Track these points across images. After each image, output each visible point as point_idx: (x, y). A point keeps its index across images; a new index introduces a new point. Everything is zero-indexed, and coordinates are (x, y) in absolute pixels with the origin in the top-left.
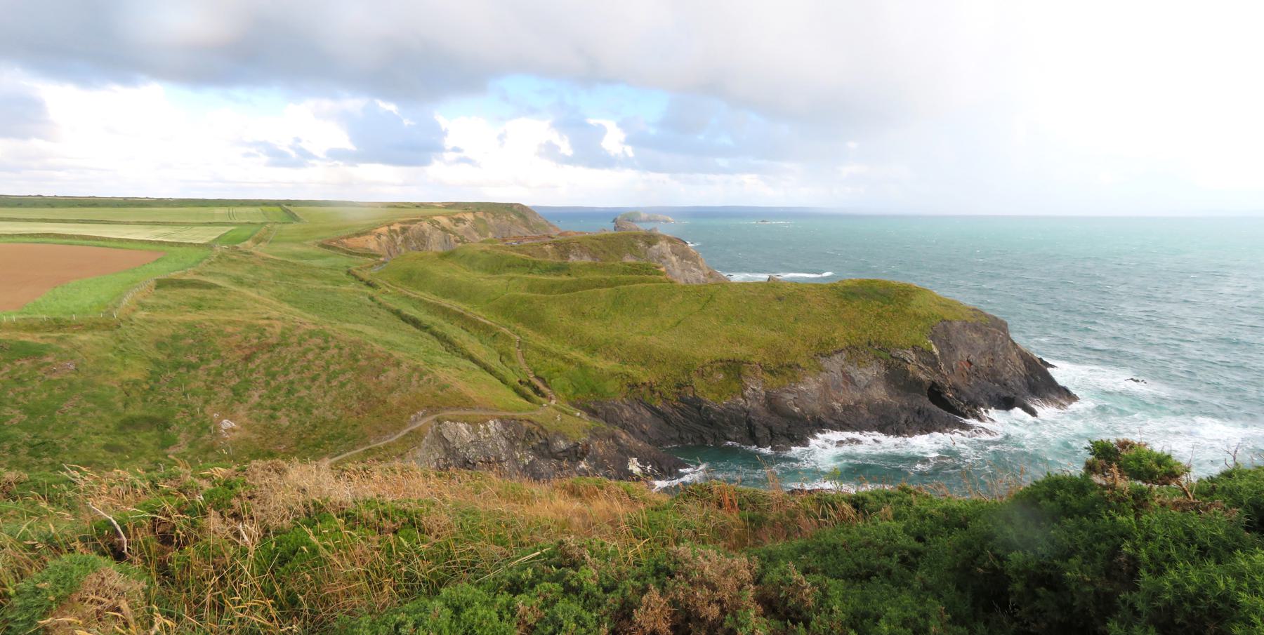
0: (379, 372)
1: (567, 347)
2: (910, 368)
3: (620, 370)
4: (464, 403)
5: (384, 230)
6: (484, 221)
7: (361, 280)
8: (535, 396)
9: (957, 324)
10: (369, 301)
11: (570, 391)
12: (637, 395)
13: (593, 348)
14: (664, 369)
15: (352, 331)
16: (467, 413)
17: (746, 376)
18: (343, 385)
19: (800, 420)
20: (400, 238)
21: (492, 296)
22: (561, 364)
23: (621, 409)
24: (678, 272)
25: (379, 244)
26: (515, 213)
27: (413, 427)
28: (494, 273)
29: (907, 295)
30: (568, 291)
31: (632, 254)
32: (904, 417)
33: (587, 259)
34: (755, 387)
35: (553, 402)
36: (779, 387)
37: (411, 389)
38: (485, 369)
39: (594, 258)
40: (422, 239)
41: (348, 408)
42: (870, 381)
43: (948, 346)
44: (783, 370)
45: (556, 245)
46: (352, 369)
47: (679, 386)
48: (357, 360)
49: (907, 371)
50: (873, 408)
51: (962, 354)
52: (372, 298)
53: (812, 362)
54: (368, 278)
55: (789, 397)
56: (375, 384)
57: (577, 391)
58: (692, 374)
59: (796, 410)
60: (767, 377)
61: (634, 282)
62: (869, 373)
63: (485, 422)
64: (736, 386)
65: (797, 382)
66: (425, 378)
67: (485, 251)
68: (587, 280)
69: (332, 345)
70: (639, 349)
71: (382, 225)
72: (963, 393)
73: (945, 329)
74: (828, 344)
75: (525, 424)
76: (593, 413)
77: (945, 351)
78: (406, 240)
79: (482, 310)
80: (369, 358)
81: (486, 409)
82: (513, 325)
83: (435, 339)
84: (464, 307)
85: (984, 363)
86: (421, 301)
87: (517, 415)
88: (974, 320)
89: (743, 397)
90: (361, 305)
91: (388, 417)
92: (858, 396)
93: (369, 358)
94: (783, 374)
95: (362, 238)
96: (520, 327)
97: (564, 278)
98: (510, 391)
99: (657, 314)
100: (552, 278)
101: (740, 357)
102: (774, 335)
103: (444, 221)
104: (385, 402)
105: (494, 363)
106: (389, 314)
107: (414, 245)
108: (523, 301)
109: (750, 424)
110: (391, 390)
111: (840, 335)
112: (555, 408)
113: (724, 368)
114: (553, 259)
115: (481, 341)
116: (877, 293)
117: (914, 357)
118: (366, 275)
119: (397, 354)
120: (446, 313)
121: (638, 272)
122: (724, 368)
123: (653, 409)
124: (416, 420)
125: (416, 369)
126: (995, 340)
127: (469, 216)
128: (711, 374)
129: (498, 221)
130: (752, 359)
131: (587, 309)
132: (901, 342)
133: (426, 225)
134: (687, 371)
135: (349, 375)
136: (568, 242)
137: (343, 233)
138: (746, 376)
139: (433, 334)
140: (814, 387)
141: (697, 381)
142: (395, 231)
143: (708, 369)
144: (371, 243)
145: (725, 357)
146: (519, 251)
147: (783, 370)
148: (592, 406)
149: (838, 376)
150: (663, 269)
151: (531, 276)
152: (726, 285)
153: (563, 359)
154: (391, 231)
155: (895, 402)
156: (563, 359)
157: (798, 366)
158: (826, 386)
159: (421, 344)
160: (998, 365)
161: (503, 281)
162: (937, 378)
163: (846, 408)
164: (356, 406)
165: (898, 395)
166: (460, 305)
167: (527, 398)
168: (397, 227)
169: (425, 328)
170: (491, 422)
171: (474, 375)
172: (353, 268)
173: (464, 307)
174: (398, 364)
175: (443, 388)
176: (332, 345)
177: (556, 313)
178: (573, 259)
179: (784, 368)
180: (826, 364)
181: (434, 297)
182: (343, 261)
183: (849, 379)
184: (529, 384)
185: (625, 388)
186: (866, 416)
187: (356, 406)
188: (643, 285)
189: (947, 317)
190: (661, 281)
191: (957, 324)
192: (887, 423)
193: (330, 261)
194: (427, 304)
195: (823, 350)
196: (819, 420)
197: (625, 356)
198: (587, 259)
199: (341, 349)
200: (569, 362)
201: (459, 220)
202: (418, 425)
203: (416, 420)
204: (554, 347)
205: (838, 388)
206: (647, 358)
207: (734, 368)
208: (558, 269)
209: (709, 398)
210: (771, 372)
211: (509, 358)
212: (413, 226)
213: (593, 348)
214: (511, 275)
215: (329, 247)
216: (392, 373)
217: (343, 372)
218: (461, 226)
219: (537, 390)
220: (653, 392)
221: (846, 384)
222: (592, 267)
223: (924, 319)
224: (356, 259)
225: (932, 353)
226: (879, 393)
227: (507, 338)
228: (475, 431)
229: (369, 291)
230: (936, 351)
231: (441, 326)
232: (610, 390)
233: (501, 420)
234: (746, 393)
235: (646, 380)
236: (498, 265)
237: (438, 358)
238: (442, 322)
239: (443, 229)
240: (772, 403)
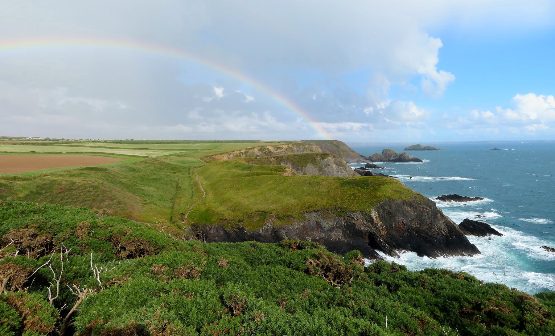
3: (222, 213)
23: (210, 229)
24: (335, 173)
34: (269, 225)
53: (300, 215)
55: (284, 231)
89: (262, 229)
113: (260, 215)
123: (225, 231)
128: (253, 217)
130: (273, 211)
140: (296, 228)
141: (246, 219)
145: (262, 210)
158: (305, 228)
179: (285, 217)
180: (308, 216)
183: (318, 225)
185: (219, 220)
205: (312, 230)
206: (235, 209)
207: (263, 214)
210: (279, 218)
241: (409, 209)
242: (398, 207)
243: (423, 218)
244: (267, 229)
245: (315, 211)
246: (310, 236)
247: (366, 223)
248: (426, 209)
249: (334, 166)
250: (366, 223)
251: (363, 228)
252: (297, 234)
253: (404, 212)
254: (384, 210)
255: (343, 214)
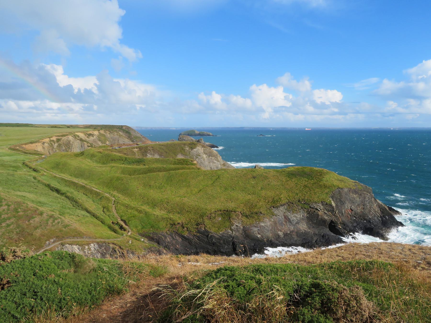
0: (30, 218)
1: (140, 204)
2: (320, 213)
3: (167, 216)
4: (79, 234)
5: (47, 140)
6: (104, 135)
7: (30, 168)
8: (119, 230)
9: (346, 190)
10: (33, 180)
11: (140, 227)
12: (174, 230)
13: (154, 204)
14: (190, 215)
15: (20, 196)
16: (79, 240)
17: (233, 219)
18: (8, 226)
19: (261, 241)
20: (56, 144)
21: (102, 176)
22: (136, 213)
25: (44, 148)
26: (124, 131)
27: (47, 248)
28: (104, 163)
29: (321, 175)
30: (142, 173)
31: (182, 154)
32: (315, 239)
33: (157, 156)
34: (238, 223)
35: (129, 234)
36: (250, 224)
37: (48, 227)
38: (94, 216)
39: (160, 155)
40: (68, 145)
41: (11, 238)
42: (299, 221)
43: (340, 202)
44: (253, 215)
45: (140, 148)
46: (14, 217)
47: (197, 225)
48: (18, 212)
49: (318, 215)
50: (299, 234)
51: (348, 205)
52: (35, 178)
53: (268, 211)
54: (33, 167)
55: (256, 229)
56: (27, 225)
57: (143, 227)
58: (204, 218)
59: (259, 236)
60: (244, 219)
61: (179, 169)
62: (298, 216)
63: (88, 244)
64: (228, 224)
65: (260, 221)
66: (56, 221)
67: (100, 152)
68: (154, 168)
69: (4, 204)
70: (178, 205)
71: (46, 137)
72: (348, 226)
73: (340, 193)
74: (277, 201)
75: (111, 246)
76: (151, 239)
77: (339, 204)
78: (59, 146)
79: (96, 184)
80: (25, 211)
81: (90, 238)
82: (112, 192)
83: (67, 200)
84: (86, 182)
85: (359, 210)
86: (62, 179)
87: (107, 240)
88: (355, 188)
89: (231, 230)
90: (28, 181)
91: (33, 242)
92: (292, 228)
93: (25, 211)
94: (253, 217)
95: (34, 145)
96: (115, 193)
97: (141, 167)
98: (106, 227)
99: (189, 186)
100: (135, 166)
101: (230, 209)
102: (250, 197)
103: (82, 135)
104: (32, 235)
105: (99, 212)
106: (44, 187)
107: (64, 148)
108: (118, 179)
109: (233, 244)
110: (36, 228)
111: (284, 197)
112: (130, 237)
113: (222, 214)
114: (138, 156)
115: (93, 201)
116: (305, 174)
117: (322, 207)
118: (33, 165)
119: (41, 209)
120: (75, 185)
121: (182, 164)
122: (222, 214)
124: (49, 244)
125: (51, 216)
126: (365, 198)
127: (96, 133)
128: (215, 218)
129: (112, 135)
130: (237, 210)
131: (152, 183)
132: (316, 200)
133: (71, 138)
134: (202, 216)
135: (13, 220)
136: (147, 147)
137: (23, 142)
138: (233, 219)
139: (67, 197)
140: (269, 224)
141: (207, 222)
142: (53, 141)
143: (213, 215)
144: (39, 147)
146: (119, 152)
147: (253, 215)
148: (151, 235)
149: (281, 218)
150: (195, 162)
151: (123, 166)
152: (226, 170)
153: (137, 210)
154: (51, 141)
155: (311, 231)
156: (137, 210)
157: (261, 213)
158: (275, 223)
159: (59, 203)
160: (367, 211)
161: (108, 168)
162: (334, 219)
163: (286, 235)
164: (15, 237)
165: (313, 227)
166: (83, 181)
167: (115, 231)
168: (54, 139)
169: (62, 194)
170: (92, 245)
171: (87, 219)
172: (27, 161)
173: (86, 182)
174: (41, 214)
175: (66, 226)
176: (4, 204)
177: (135, 184)
178: (149, 156)
180: (276, 212)
181: (70, 177)
182: (22, 157)
183: (287, 219)
184: (117, 224)
185: (169, 225)
186: (295, 239)
187: (15, 237)
188: (183, 171)
189: (340, 186)
190: (193, 169)
191: (346, 190)
192: (307, 243)
193: (13, 158)
194: (66, 181)
195: (274, 204)
196: (271, 241)
197: (170, 209)
198: (157, 156)
199: (9, 206)
200: (140, 212)
201: (90, 135)
202: (50, 247)
203: (49, 244)
204: (133, 204)
205: (281, 224)
206: (181, 209)
207: (227, 214)
208: (139, 162)
209: (213, 231)
210: (247, 216)
211: (108, 210)
212: (63, 138)
213: (154, 204)
214: (113, 165)
215: (14, 150)
216: (37, 219)
217: (9, 219)
218: (91, 138)
219: (121, 228)
220: (183, 227)
221: (286, 222)
222: (157, 161)
223: (329, 188)
224: (29, 156)
225: (331, 205)
226: (303, 227)
227: (108, 199)
228: (83, 249)
229: (34, 174)
230: (333, 204)
231: (72, 193)
232: (161, 227)
233: (98, 243)
234: (233, 228)
235: (180, 221)
236: (106, 159)
237: (68, 211)
238: (72, 190)
239: (81, 140)
240: (247, 234)
241: (355, 196)
242: (346, 194)
243: (365, 203)
244: (237, 229)
245: (281, 205)
246: (281, 231)
247: (326, 212)
248: (367, 195)
249: (205, 156)
250: (326, 212)
251: (326, 218)
252: (271, 230)
253: (351, 199)
254: (336, 199)
255: (306, 206)
